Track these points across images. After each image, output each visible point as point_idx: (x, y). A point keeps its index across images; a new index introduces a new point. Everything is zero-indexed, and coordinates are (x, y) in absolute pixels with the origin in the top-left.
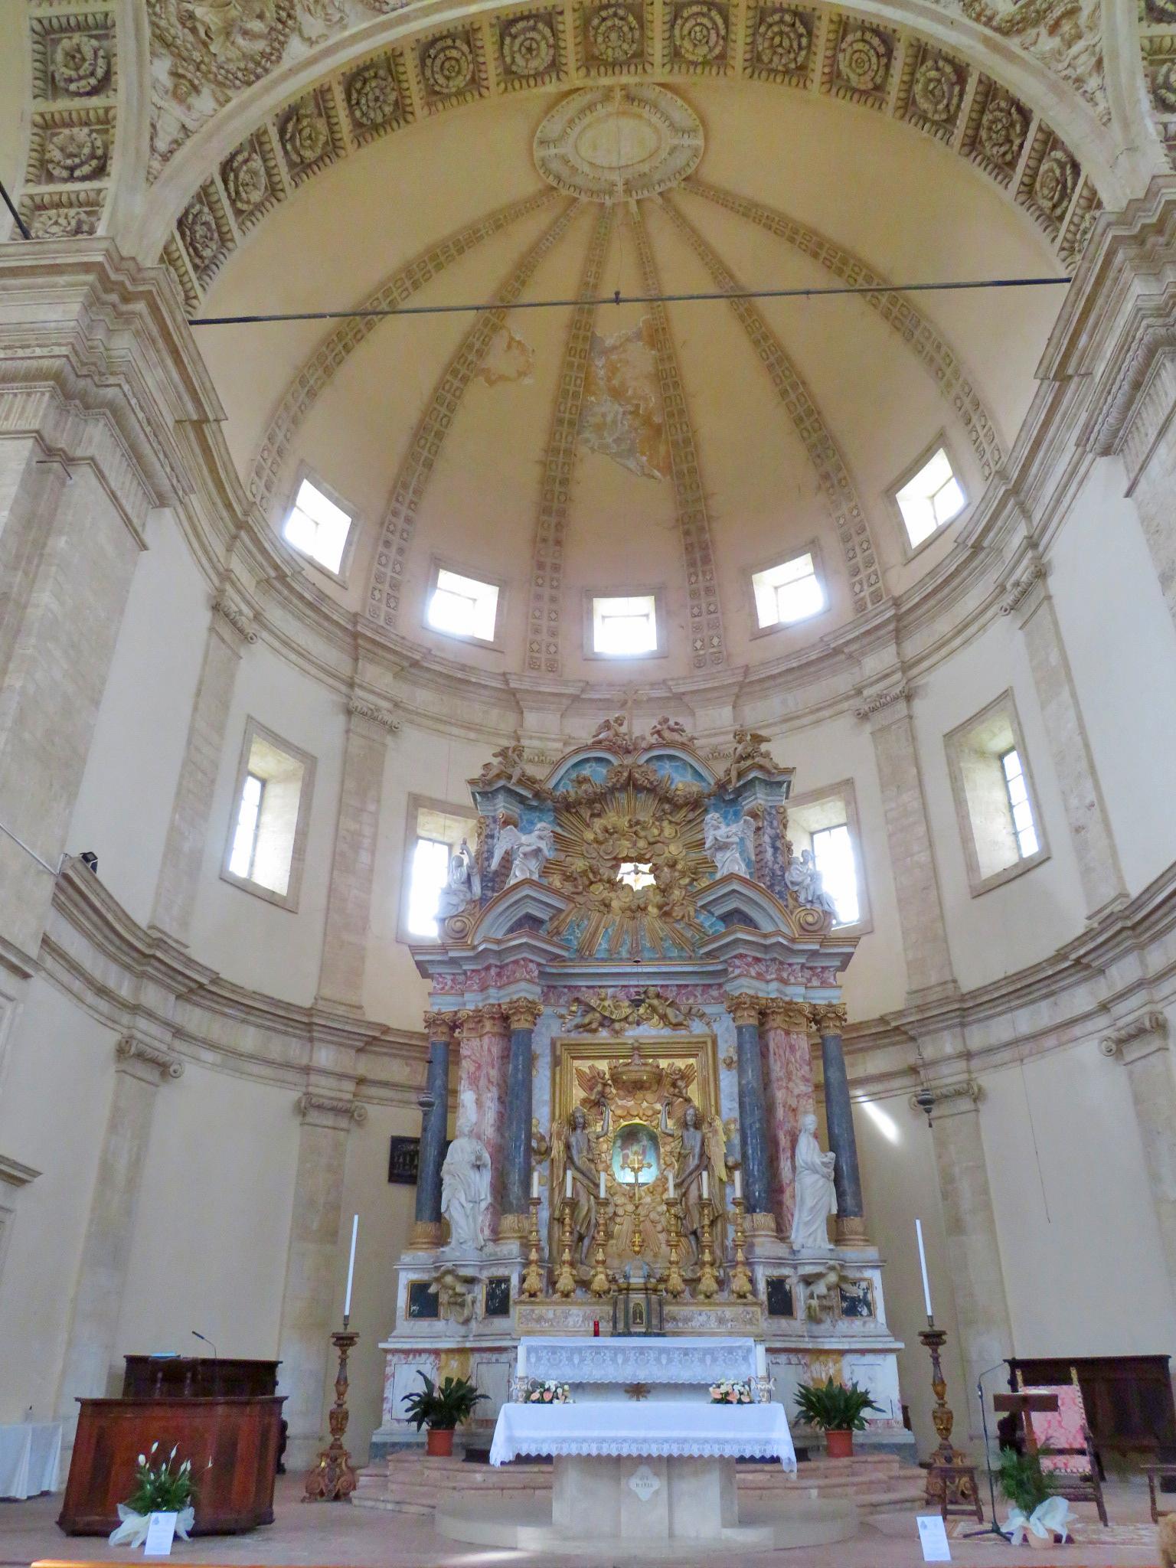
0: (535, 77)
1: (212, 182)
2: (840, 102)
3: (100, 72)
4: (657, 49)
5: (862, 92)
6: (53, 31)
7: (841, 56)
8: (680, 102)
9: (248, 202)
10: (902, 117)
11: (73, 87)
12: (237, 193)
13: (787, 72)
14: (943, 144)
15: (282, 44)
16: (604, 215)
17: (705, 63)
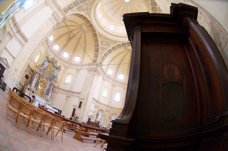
16: (80, 29)
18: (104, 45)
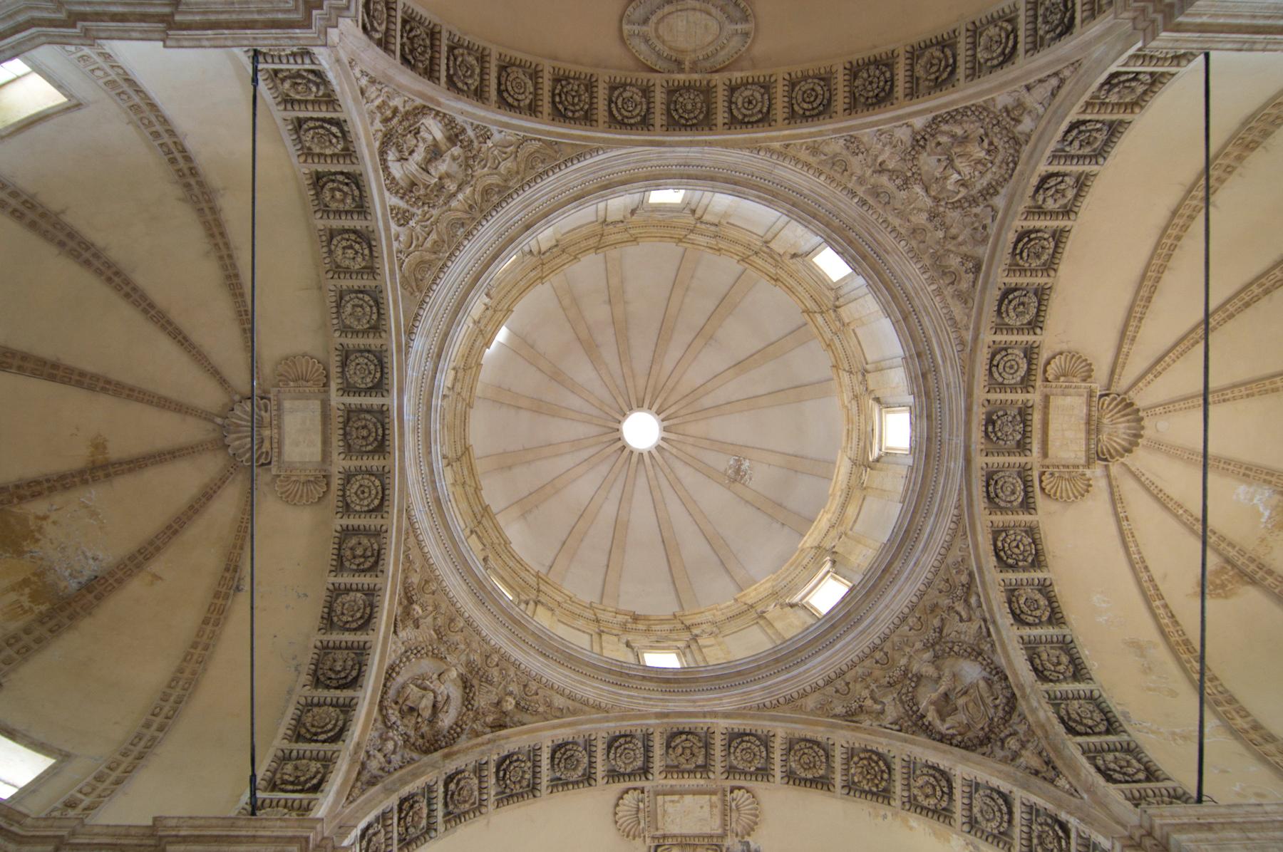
0: (748, 83)
1: (1027, 52)
2: (529, 58)
3: (1074, 133)
4: (659, 97)
5: (514, 65)
6: (1091, 157)
7: (532, 90)
8: (641, 58)
9: (1001, 28)
10: (484, 49)
11: (1099, 126)
12: (1008, 37)
13: (567, 78)
14: (455, 31)
15: (930, 126)
17: (624, 86)
18: (435, 153)
